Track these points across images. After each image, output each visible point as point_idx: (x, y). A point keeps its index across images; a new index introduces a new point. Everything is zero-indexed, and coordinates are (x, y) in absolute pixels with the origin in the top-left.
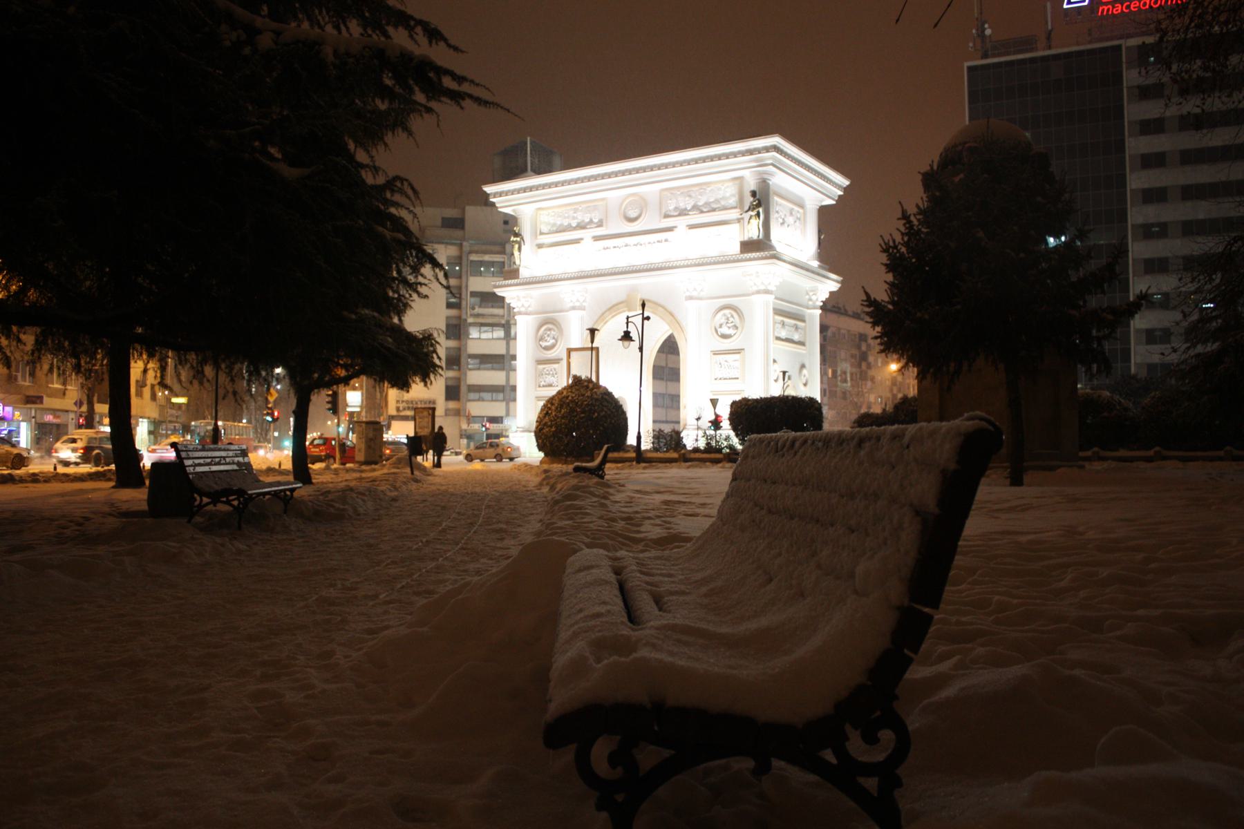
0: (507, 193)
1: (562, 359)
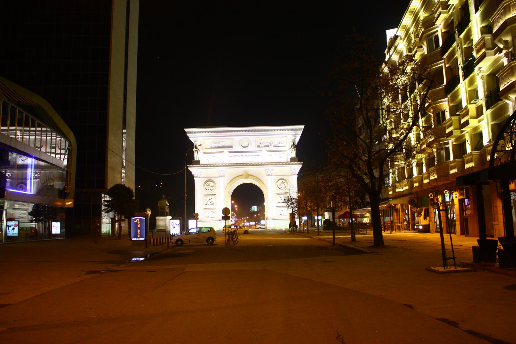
0: (192, 133)
1: (216, 195)
